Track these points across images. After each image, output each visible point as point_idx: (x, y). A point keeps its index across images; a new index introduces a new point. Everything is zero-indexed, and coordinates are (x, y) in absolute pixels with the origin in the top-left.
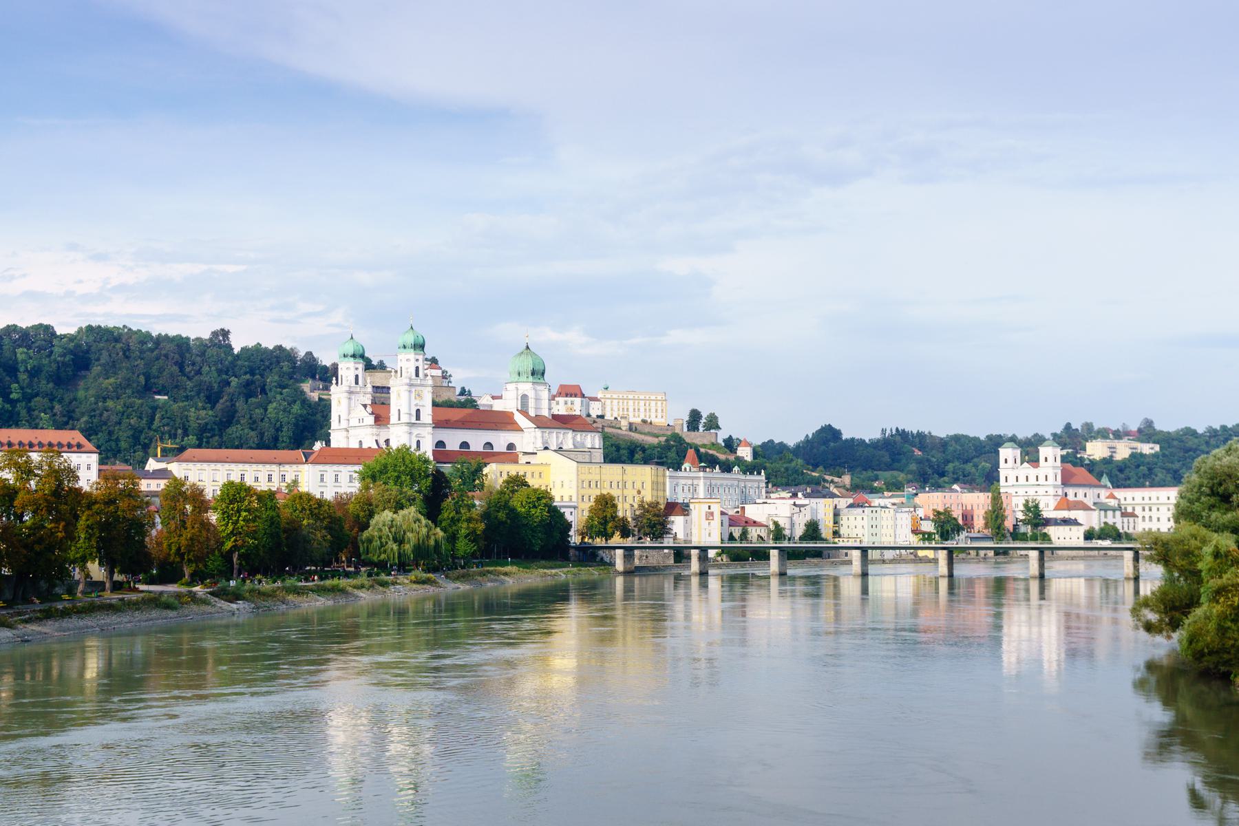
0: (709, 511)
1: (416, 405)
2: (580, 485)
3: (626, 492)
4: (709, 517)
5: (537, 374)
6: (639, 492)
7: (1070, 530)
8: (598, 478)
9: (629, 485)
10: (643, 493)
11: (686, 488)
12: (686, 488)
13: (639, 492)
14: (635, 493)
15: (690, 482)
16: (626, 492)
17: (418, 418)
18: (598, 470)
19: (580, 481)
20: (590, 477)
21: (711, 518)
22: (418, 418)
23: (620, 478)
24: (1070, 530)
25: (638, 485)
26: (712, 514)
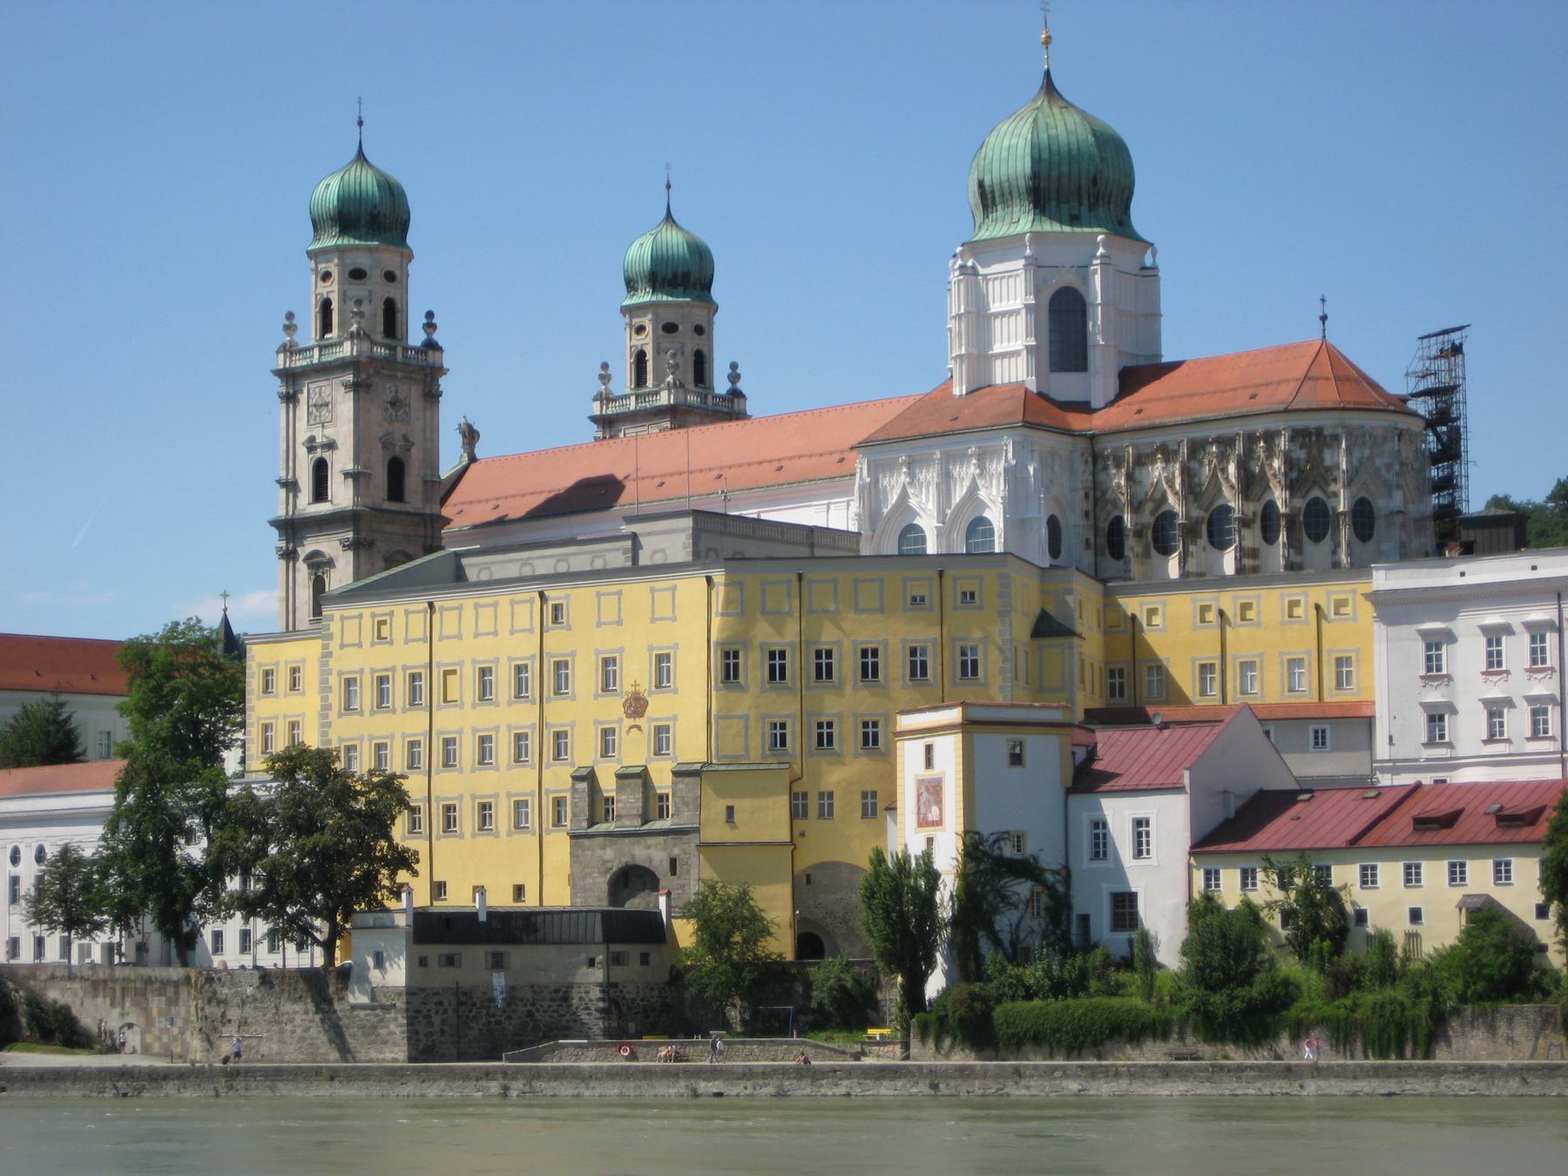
0: (929, 774)
2: (336, 698)
3: (559, 713)
4: (929, 808)
6: (636, 706)
7: (519, 891)
8: (416, 657)
9: (584, 676)
10: (658, 707)
13: (636, 706)
14: (612, 710)
16: (559, 713)
19: (335, 682)
23: (526, 648)
24: (519, 891)
25: (635, 673)
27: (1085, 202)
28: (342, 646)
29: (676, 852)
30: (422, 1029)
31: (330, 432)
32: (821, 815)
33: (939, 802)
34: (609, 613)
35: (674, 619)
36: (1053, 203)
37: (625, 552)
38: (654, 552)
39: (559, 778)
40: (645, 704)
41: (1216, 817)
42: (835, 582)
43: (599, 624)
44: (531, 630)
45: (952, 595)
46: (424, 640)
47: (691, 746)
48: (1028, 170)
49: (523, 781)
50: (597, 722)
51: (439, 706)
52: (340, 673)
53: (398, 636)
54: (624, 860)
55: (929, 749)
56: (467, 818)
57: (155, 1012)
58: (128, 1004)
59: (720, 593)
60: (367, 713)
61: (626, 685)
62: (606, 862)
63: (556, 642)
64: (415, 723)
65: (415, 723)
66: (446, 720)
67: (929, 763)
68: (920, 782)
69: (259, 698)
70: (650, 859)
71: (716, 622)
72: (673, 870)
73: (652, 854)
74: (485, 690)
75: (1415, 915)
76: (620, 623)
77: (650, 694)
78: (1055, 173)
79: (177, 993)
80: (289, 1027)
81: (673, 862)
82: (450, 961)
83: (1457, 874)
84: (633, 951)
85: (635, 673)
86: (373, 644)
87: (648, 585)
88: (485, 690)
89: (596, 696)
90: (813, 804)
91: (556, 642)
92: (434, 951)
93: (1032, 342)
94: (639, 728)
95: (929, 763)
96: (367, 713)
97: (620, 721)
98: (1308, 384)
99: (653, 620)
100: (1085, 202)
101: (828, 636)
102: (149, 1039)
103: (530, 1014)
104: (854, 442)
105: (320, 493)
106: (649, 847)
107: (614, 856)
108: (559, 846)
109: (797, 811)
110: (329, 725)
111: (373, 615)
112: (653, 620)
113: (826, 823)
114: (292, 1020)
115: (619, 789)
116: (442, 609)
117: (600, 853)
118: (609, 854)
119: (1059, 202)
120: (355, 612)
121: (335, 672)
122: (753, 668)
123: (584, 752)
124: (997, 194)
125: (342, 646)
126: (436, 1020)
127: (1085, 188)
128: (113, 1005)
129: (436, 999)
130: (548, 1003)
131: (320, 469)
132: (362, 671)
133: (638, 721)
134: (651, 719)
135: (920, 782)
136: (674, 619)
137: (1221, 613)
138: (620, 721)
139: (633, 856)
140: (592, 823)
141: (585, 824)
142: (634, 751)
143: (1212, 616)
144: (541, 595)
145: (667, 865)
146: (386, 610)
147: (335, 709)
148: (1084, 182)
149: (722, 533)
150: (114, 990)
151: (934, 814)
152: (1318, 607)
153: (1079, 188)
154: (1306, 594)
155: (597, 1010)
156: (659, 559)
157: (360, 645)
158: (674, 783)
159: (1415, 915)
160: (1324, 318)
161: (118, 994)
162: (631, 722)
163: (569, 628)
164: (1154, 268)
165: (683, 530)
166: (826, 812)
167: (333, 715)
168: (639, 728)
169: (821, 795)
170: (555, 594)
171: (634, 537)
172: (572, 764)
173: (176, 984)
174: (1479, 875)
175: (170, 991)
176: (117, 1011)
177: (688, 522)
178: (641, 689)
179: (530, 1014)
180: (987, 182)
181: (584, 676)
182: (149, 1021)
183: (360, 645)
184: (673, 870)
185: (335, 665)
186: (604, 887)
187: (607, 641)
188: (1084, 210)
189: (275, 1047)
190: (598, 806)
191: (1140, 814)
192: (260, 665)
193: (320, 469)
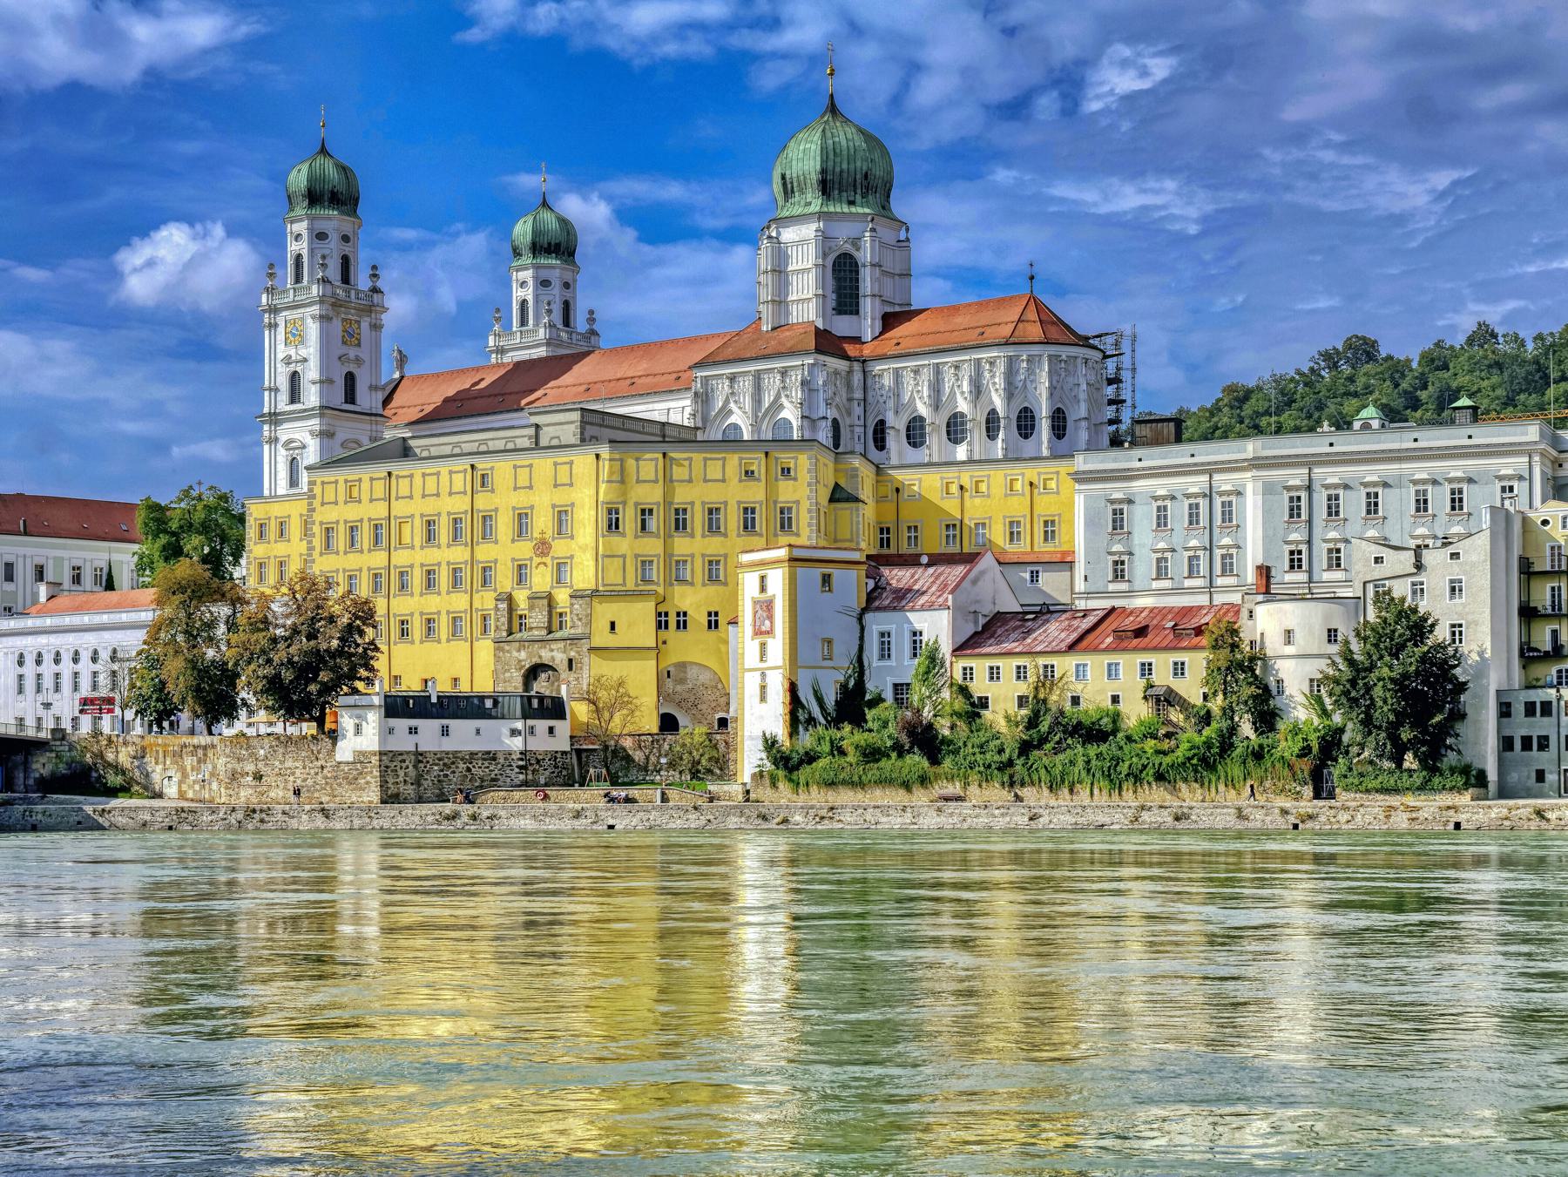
0: (763, 596)
1: (288, 361)
5: (802, 192)
6: (543, 548)
8: (379, 510)
9: (504, 526)
10: (560, 548)
11: (1178, 513)
12: (1178, 513)
13: (543, 548)
14: (525, 550)
15: (1196, 484)
17: (350, 397)
20: (352, 513)
22: (350, 397)
23: (460, 504)
25: (542, 523)
26: (768, 606)
27: (859, 191)
28: (323, 504)
29: (572, 654)
30: (391, 780)
31: (303, 352)
32: (678, 627)
33: (771, 618)
34: (523, 479)
35: (571, 485)
36: (836, 192)
37: (530, 438)
38: (552, 438)
39: (486, 600)
41: (969, 630)
42: (690, 459)
43: (516, 488)
44: (465, 493)
46: (384, 500)
47: (584, 575)
48: (818, 167)
49: (460, 602)
50: (513, 560)
51: (395, 548)
52: (321, 523)
53: (365, 497)
54: (535, 660)
55: (763, 578)
56: (417, 628)
57: (189, 768)
58: (168, 762)
59: (605, 466)
60: (341, 553)
62: (520, 661)
63: (483, 502)
64: (378, 559)
66: (401, 558)
67: (763, 589)
69: (255, 544)
70: (553, 658)
71: (603, 487)
72: (570, 668)
73: (555, 655)
74: (430, 536)
76: (531, 487)
77: (554, 539)
78: (838, 169)
79: (205, 755)
80: (291, 778)
81: (570, 661)
82: (413, 731)
83: (1146, 669)
84: (542, 725)
85: (542, 523)
86: (346, 502)
87: (550, 462)
89: (513, 541)
91: (483, 502)
92: (402, 724)
93: (820, 292)
94: (545, 564)
95: (763, 589)
96: (341, 553)
97: (531, 559)
98: (1020, 325)
99: (556, 486)
100: (859, 191)
101: (682, 496)
102: (184, 787)
103: (469, 770)
104: (692, 364)
105: (294, 397)
106: (552, 650)
107: (526, 658)
108: (485, 649)
109: (662, 624)
110: (313, 561)
111: (346, 481)
112: (556, 486)
113: (682, 634)
114: (293, 774)
115: (531, 608)
116: (398, 477)
118: (523, 655)
119: (840, 191)
120: (333, 479)
121: (317, 523)
122: (629, 520)
124: (795, 184)
125: (323, 504)
126: (401, 773)
127: (859, 181)
128: (157, 763)
129: (400, 758)
130: (480, 762)
131: (294, 378)
132: (337, 522)
133: (544, 560)
134: (553, 558)
136: (571, 485)
137: (962, 488)
138: (531, 559)
139: (540, 657)
140: (510, 634)
141: (505, 634)
142: (541, 579)
143: (954, 489)
144: (473, 467)
145: (566, 663)
146: (356, 477)
147: (318, 550)
148: (858, 177)
149: (601, 426)
150: (157, 752)
152: (1031, 484)
153: (855, 180)
154: (1023, 474)
155: (518, 767)
156: (555, 442)
158: (572, 605)
160: (1032, 278)
161: (161, 755)
162: (538, 560)
163: (493, 491)
164: (908, 240)
165: (572, 422)
166: (682, 625)
167: (316, 554)
168: (545, 564)
169: (678, 614)
170: (483, 464)
171: (537, 426)
172: (495, 590)
173: (205, 748)
176: (159, 768)
177: (576, 416)
179: (469, 770)
180: (788, 177)
181: (504, 526)
182: (185, 775)
184: (570, 668)
185: (317, 517)
186: (520, 679)
187: (521, 499)
188: (858, 197)
189: (281, 794)
190: (515, 623)
192: (256, 519)
193: (294, 378)
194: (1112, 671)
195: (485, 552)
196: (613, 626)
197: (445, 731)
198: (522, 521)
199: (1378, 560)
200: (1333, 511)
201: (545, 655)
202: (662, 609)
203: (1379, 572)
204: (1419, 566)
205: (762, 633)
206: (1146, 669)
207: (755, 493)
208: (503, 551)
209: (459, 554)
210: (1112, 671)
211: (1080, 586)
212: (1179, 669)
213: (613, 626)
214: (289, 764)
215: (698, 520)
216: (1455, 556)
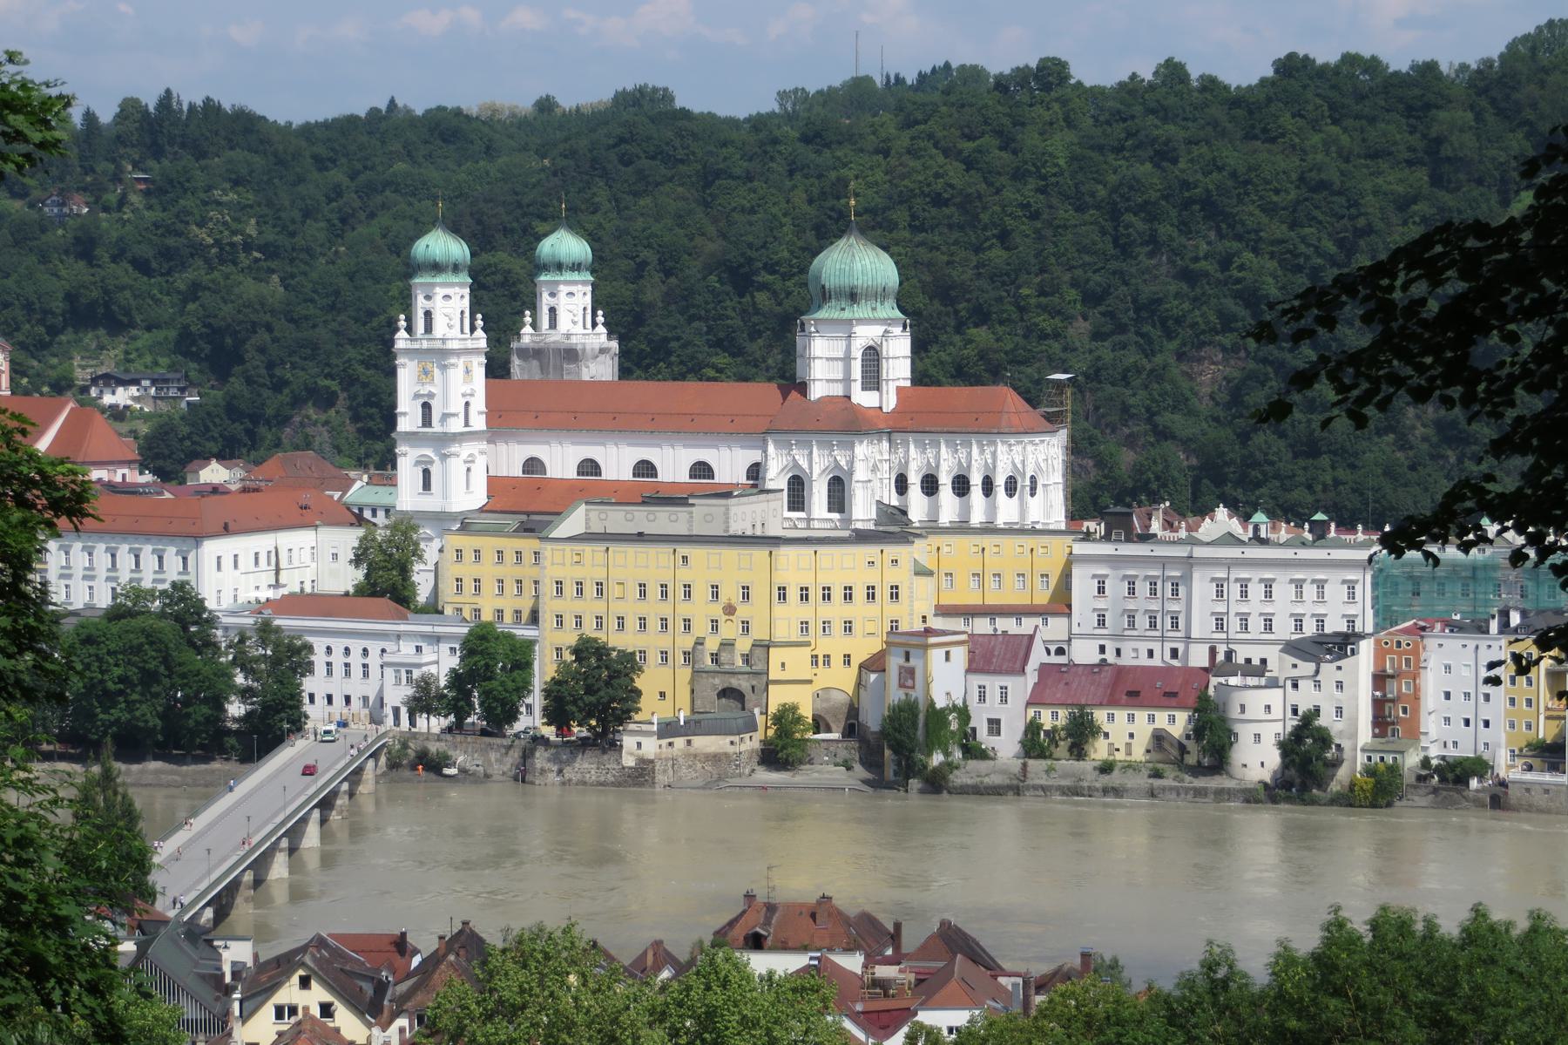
0: (906, 665)
4: (906, 680)
6: (730, 610)
8: (600, 575)
9: (701, 592)
10: (743, 611)
13: (730, 610)
14: (716, 610)
18: (600, 557)
20: (579, 573)
21: (910, 683)
25: (730, 593)
28: (553, 564)
29: (754, 683)
40: (735, 609)
44: (669, 567)
45: (887, 562)
54: (726, 685)
61: (723, 598)
64: (599, 607)
65: (599, 607)
66: (618, 608)
68: (901, 667)
75: (1131, 736)
81: (753, 687)
83: (1152, 719)
88: (643, 594)
90: (821, 660)
91: (684, 575)
117: (711, 680)
118: (717, 681)
123: (701, 628)
125: (553, 564)
135: (901, 667)
142: (729, 630)
151: (910, 683)
157: (564, 564)
159: (1131, 736)
170: (683, 550)
174: (1161, 719)
175: (503, 751)
178: (733, 602)
181: (701, 592)
183: (564, 564)
191: (1003, 684)
194: (1131, 718)
195: (684, 609)
196: (783, 665)
197: (689, 742)
198: (715, 592)
199: (1295, 666)
200: (1244, 594)
201: (735, 682)
202: (814, 653)
203: (1295, 673)
204: (1317, 672)
205: (905, 687)
206: (1152, 719)
207: (872, 577)
208: (701, 610)
209: (665, 609)
210: (1131, 718)
211: (1075, 630)
212: (1172, 719)
213: (783, 665)
214: (586, 765)
215: (838, 594)
216: (1339, 668)
